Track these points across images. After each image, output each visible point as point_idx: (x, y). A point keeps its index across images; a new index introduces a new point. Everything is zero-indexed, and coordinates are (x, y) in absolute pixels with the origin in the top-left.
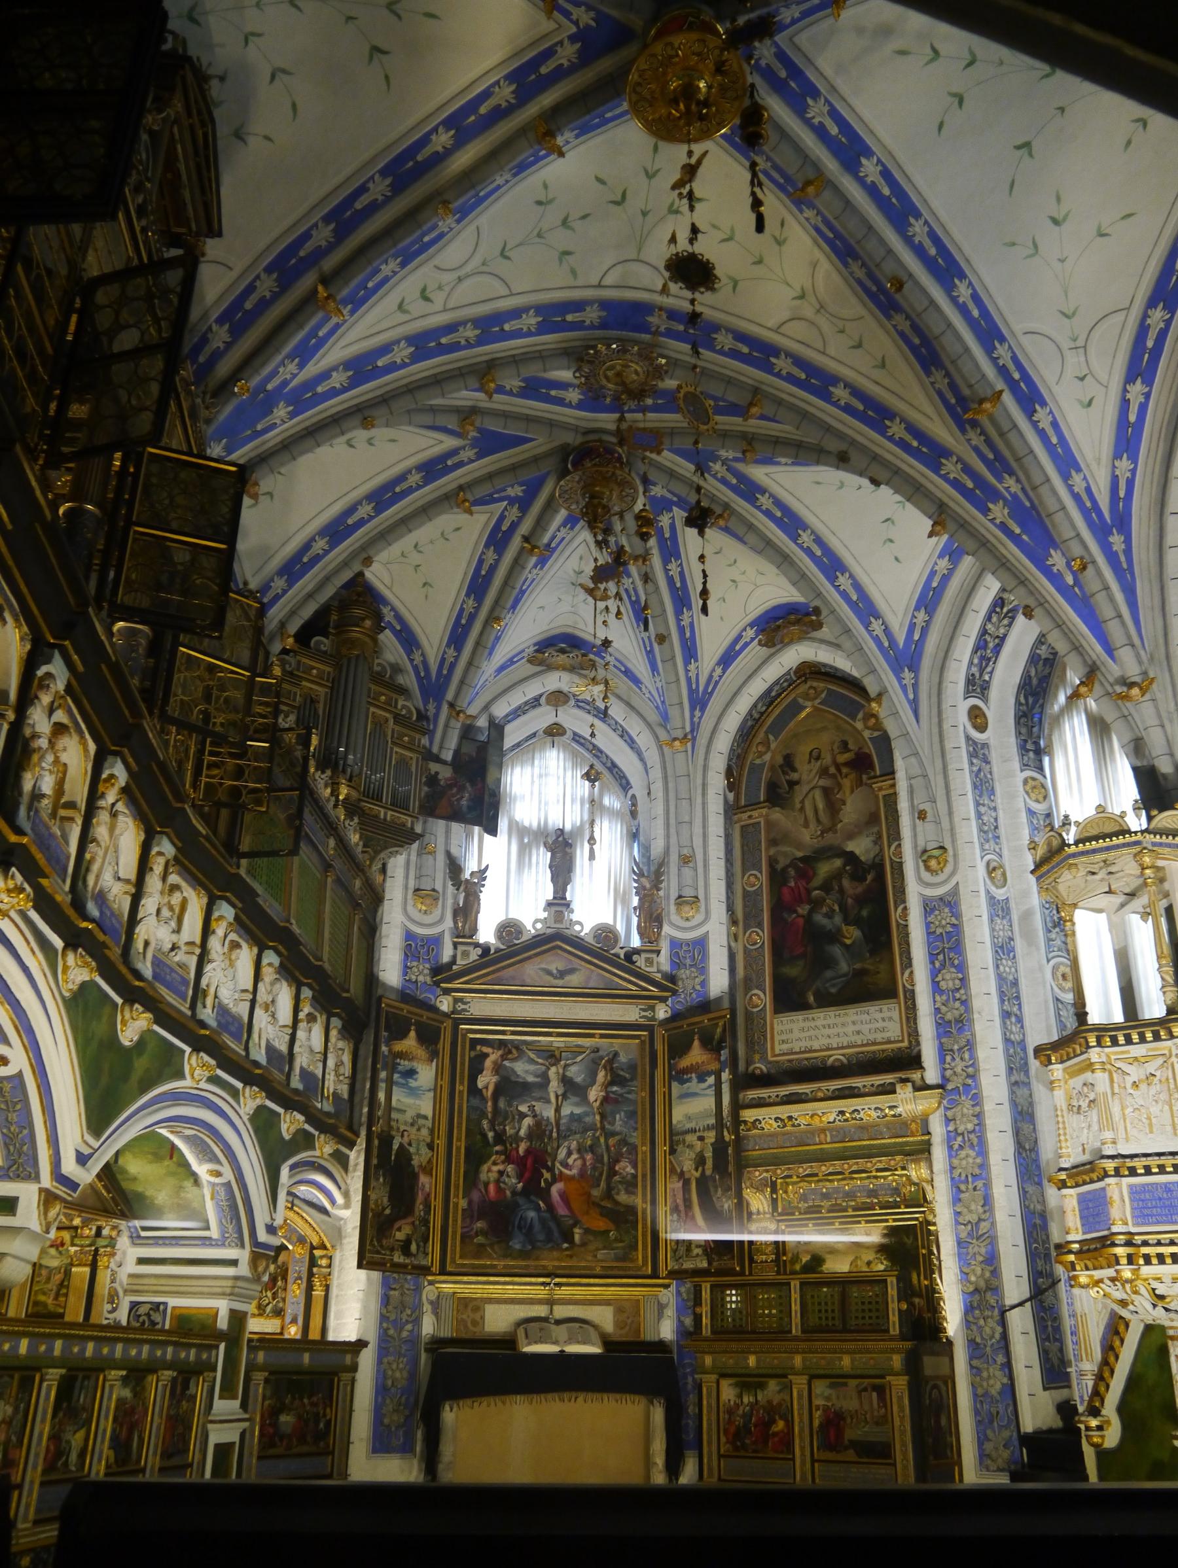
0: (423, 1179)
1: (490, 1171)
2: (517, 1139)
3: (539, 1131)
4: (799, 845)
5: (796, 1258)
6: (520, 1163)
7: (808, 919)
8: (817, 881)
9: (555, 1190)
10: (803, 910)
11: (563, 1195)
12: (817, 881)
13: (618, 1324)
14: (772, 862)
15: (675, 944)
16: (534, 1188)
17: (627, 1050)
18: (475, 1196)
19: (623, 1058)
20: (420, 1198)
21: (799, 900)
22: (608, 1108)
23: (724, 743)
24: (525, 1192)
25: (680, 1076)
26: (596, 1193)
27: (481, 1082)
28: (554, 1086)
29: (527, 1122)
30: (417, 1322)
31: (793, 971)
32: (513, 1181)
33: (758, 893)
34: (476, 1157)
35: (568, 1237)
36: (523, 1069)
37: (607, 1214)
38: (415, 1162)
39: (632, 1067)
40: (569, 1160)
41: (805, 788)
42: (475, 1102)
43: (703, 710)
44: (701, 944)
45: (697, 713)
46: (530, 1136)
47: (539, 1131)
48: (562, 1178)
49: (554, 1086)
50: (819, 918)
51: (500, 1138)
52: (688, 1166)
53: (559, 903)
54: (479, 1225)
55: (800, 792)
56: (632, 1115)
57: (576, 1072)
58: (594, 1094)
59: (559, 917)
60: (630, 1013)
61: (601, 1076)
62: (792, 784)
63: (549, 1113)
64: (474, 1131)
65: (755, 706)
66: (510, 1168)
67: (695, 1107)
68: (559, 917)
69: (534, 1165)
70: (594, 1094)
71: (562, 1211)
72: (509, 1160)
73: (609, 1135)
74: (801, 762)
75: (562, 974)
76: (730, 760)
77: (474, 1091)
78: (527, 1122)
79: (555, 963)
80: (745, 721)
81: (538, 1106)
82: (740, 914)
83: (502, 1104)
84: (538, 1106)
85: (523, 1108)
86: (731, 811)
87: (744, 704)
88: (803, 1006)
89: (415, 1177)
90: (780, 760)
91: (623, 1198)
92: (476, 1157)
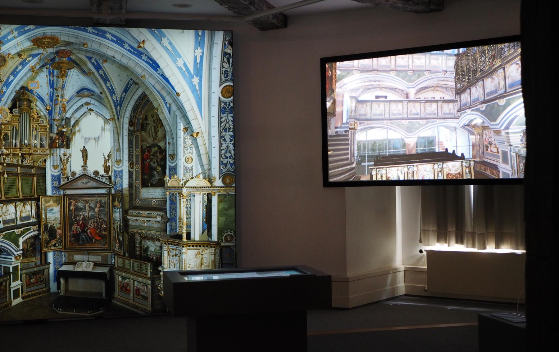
0: (58, 231)
1: (74, 227)
2: (80, 220)
3: (84, 219)
4: (148, 143)
5: (144, 246)
6: (81, 226)
7: (149, 163)
8: (152, 153)
9: (88, 231)
10: (148, 161)
11: (90, 232)
12: (152, 153)
13: (102, 260)
14: (142, 147)
15: (115, 171)
16: (84, 231)
17: (104, 200)
18: (71, 233)
19: (103, 201)
20: (58, 235)
21: (148, 158)
22: (100, 213)
23: (128, 115)
24: (82, 232)
25: (114, 206)
26: (97, 232)
27: (71, 208)
28: (87, 208)
29: (82, 216)
30: (61, 258)
31: (146, 177)
32: (79, 230)
33: (138, 155)
34: (71, 225)
35: (92, 241)
36: (80, 205)
37: (100, 236)
38: (56, 228)
39: (105, 203)
40: (91, 225)
41: (150, 126)
42: (70, 212)
43: (121, 106)
44: (122, 171)
45: (118, 108)
46: (82, 220)
47: (84, 219)
48: (90, 228)
49: (87, 208)
50: (152, 163)
51: (76, 220)
52: (116, 228)
53: (85, 166)
54: (73, 239)
55: (149, 126)
56: (105, 214)
57: (92, 205)
58: (96, 210)
59: (85, 170)
60: (103, 191)
61: (98, 205)
62: (147, 124)
63: (86, 214)
64: (70, 219)
65: (137, 101)
66: (78, 227)
67: (117, 215)
68: (85, 170)
69: (84, 226)
70: (96, 210)
71: (90, 235)
72: (78, 225)
73: (100, 219)
74: (149, 118)
75: (86, 183)
76: (130, 118)
77: (70, 210)
78: (82, 216)
79: (85, 180)
80: (134, 106)
81: (84, 213)
82: (134, 160)
83: (76, 213)
84: (84, 213)
85: (81, 214)
86: (130, 133)
87: (133, 102)
88: (148, 187)
89: (56, 231)
90: (144, 117)
91: (103, 233)
92: (71, 225)
